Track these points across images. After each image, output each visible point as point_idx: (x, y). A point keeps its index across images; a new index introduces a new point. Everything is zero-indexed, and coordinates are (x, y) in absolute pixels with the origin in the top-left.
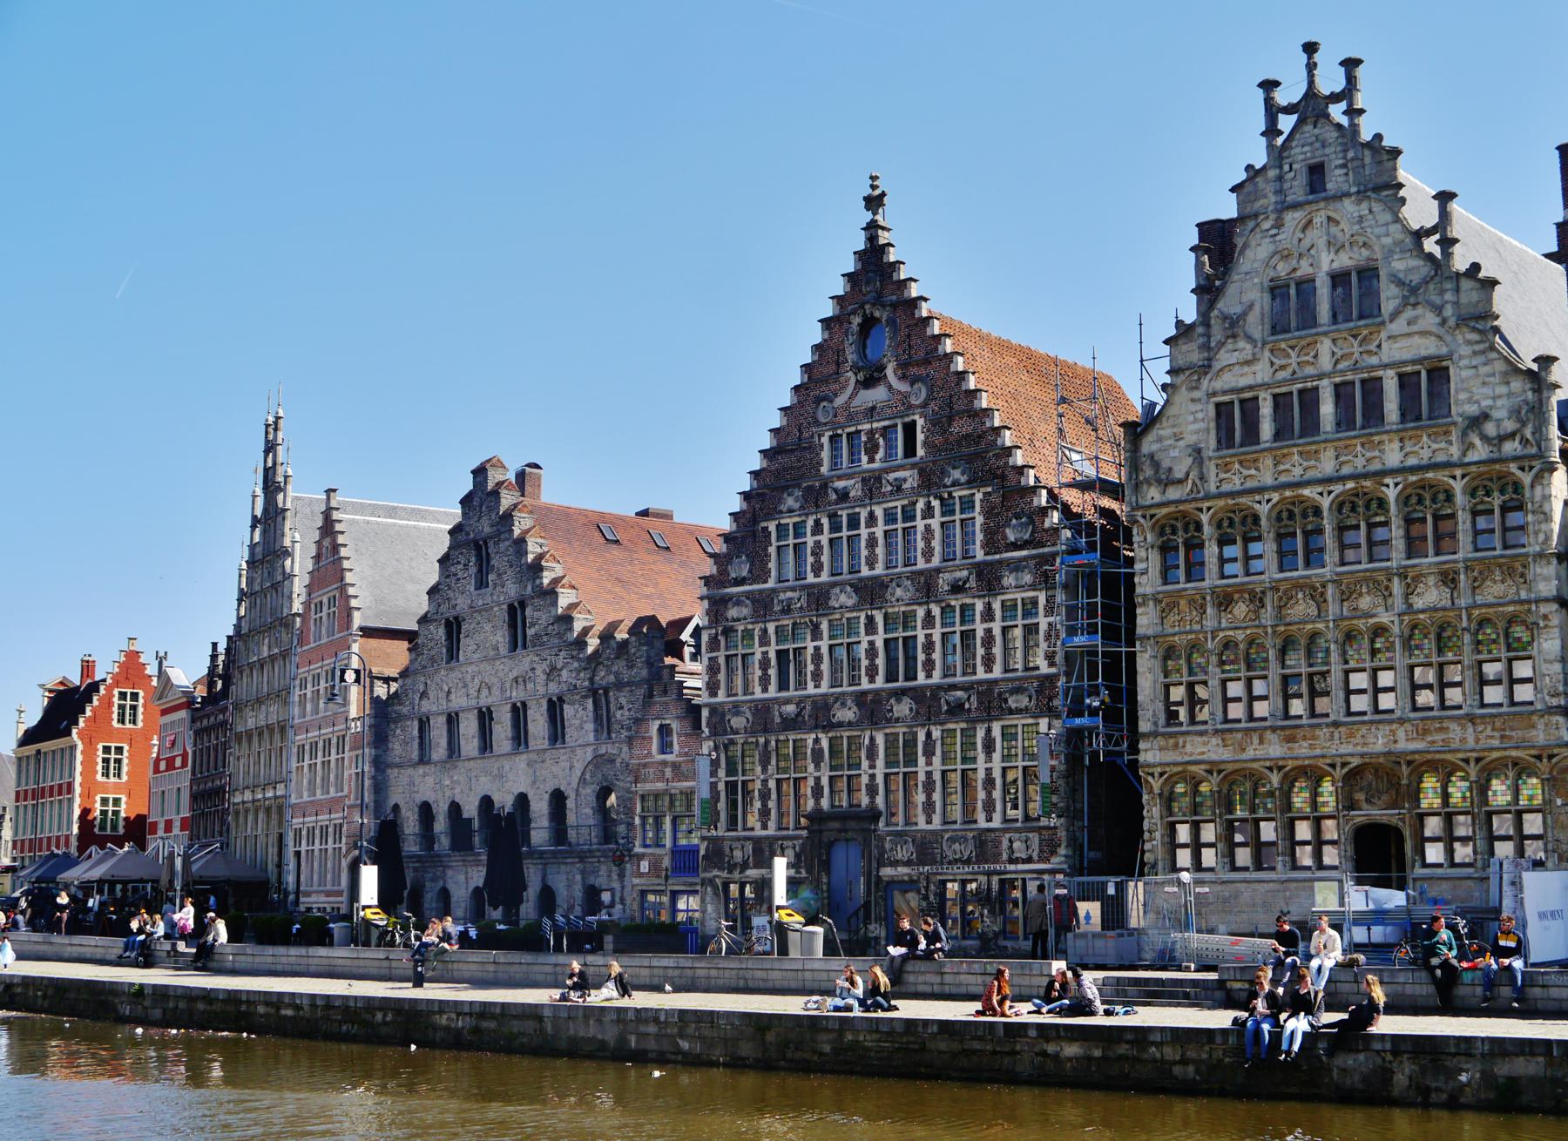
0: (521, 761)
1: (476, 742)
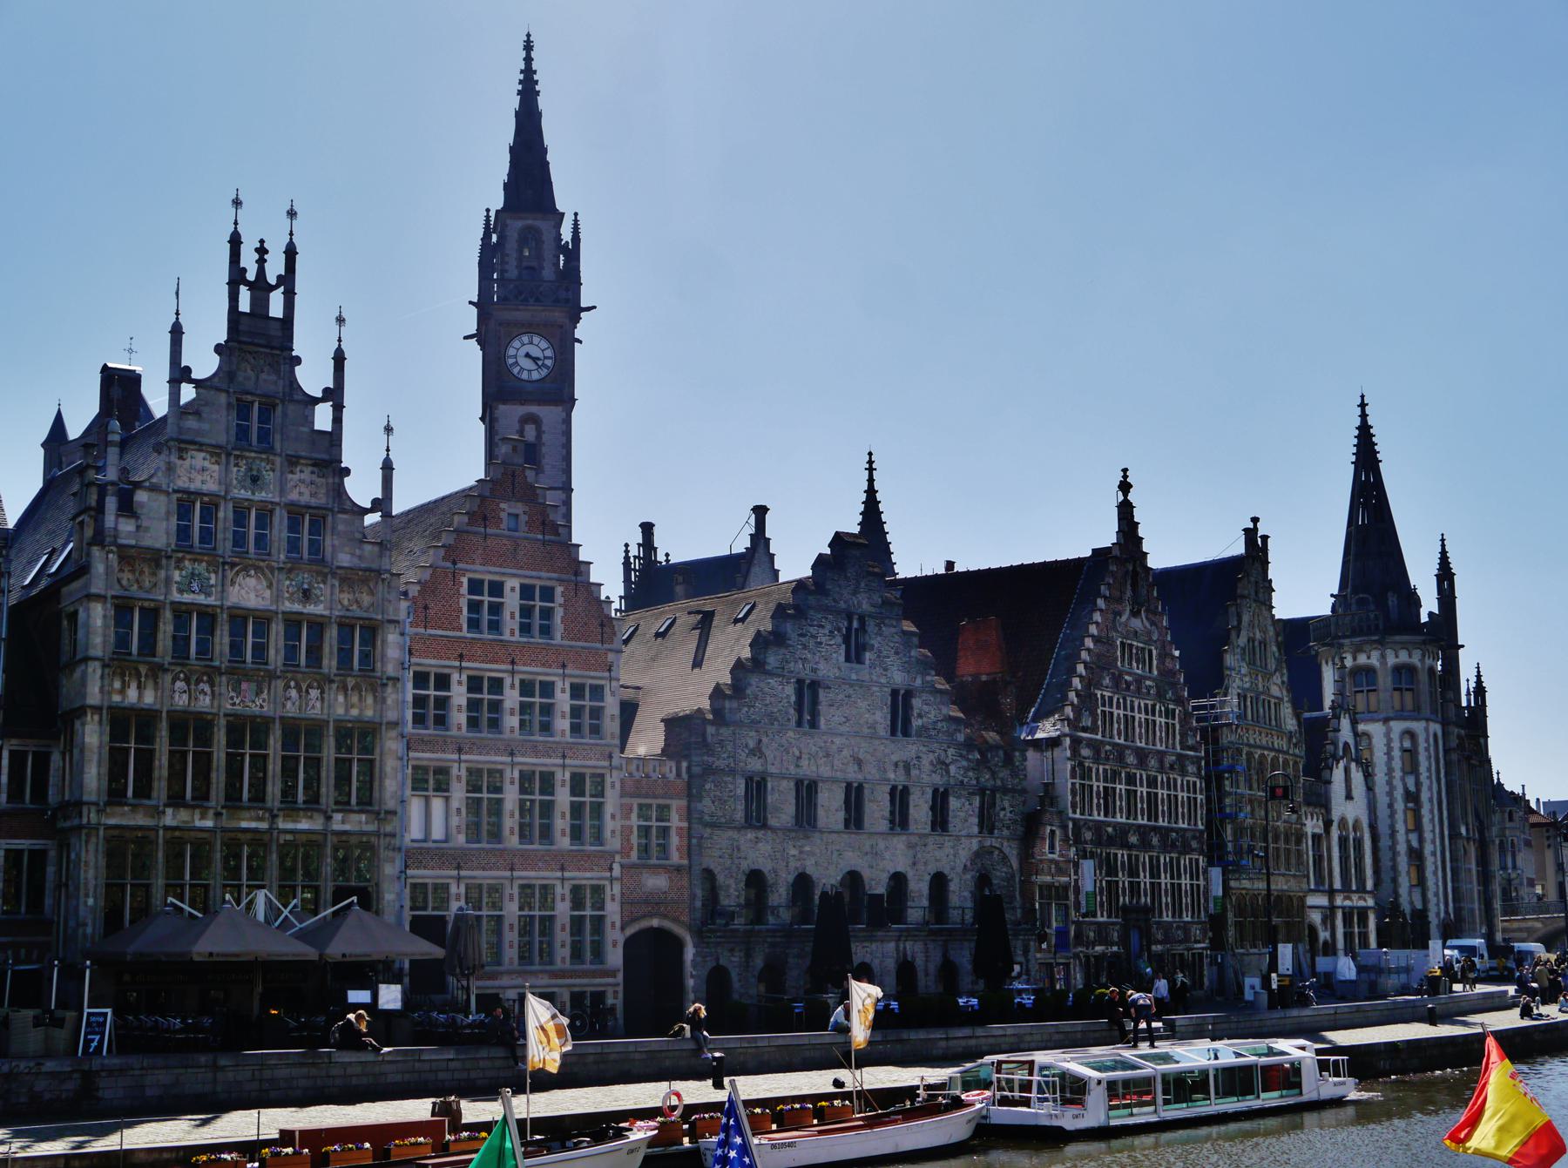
0: (899, 842)
1: (841, 815)
